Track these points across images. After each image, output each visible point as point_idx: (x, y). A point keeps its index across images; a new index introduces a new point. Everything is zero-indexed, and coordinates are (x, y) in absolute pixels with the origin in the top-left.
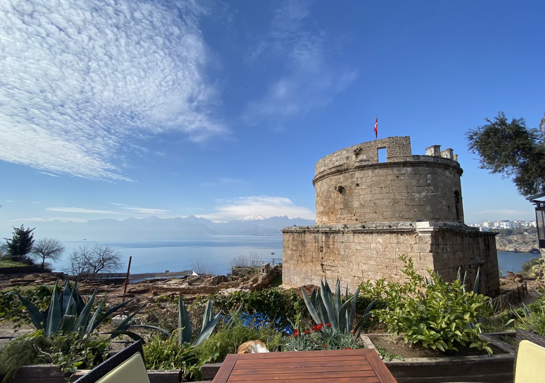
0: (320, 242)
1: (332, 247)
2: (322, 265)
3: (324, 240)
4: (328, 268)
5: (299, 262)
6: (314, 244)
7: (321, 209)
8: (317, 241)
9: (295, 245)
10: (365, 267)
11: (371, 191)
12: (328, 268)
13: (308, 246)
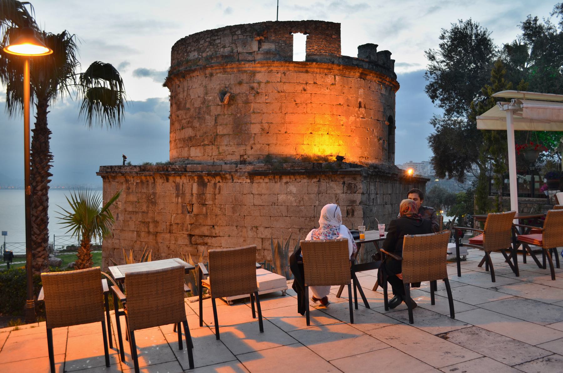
1: (211, 202)
2: (191, 236)
3: (195, 191)
4: (200, 240)
5: (143, 234)
6: (174, 200)
9: (132, 203)
11: (281, 108)
12: (200, 240)
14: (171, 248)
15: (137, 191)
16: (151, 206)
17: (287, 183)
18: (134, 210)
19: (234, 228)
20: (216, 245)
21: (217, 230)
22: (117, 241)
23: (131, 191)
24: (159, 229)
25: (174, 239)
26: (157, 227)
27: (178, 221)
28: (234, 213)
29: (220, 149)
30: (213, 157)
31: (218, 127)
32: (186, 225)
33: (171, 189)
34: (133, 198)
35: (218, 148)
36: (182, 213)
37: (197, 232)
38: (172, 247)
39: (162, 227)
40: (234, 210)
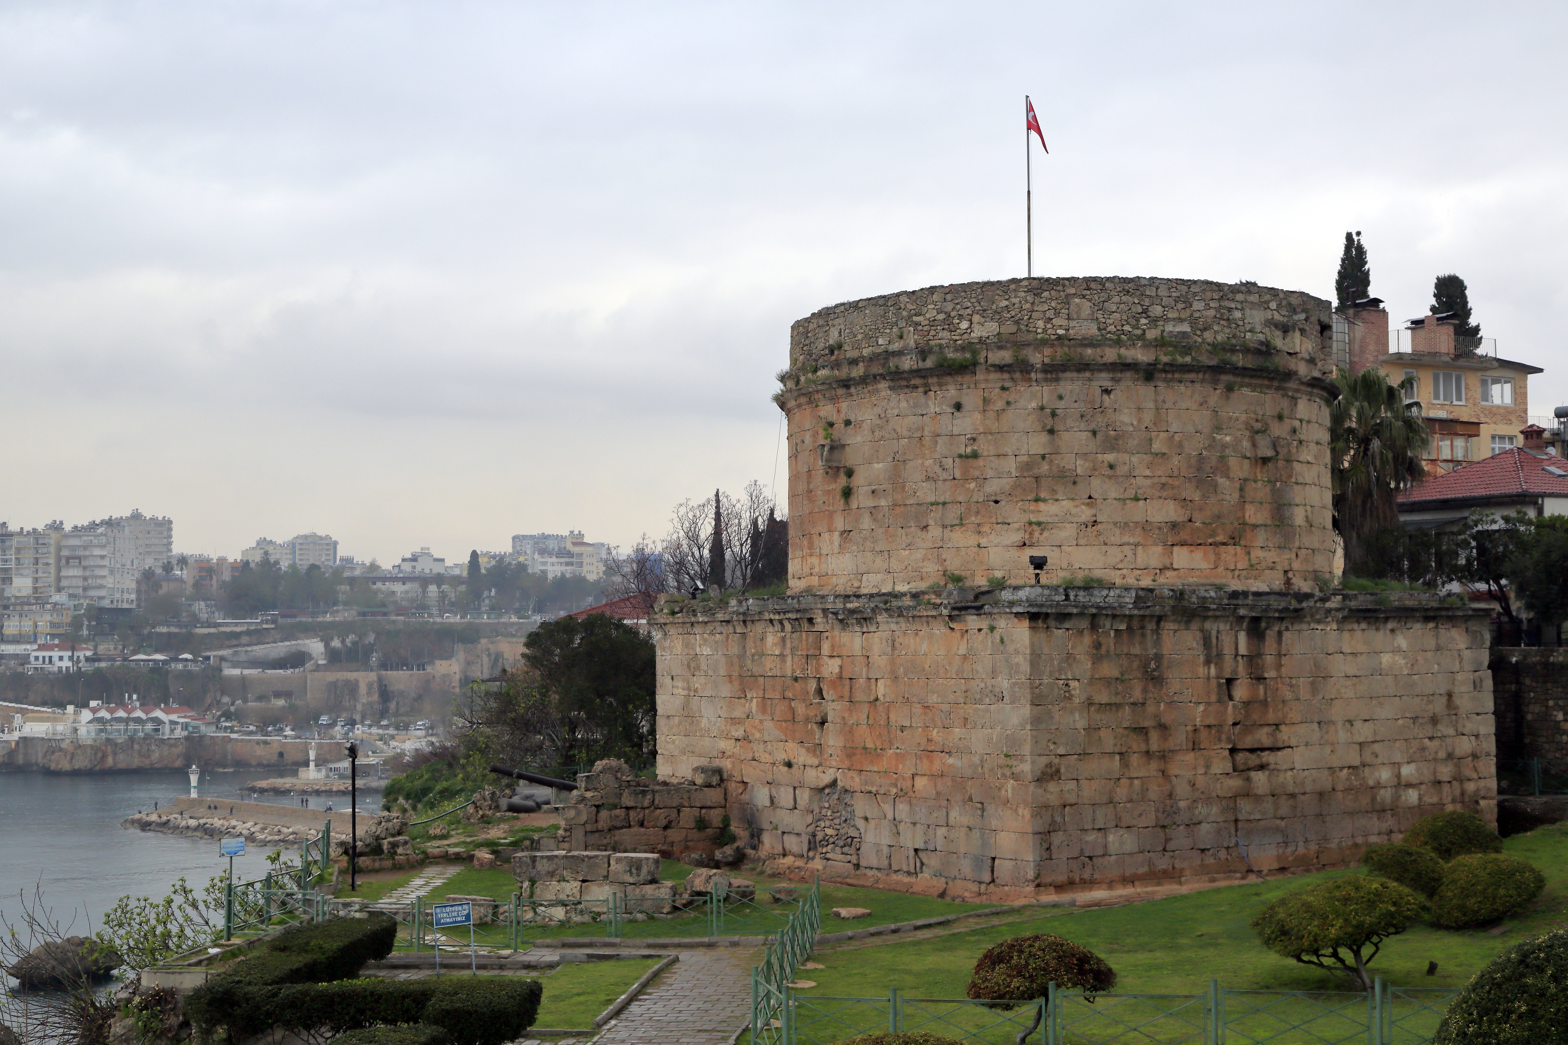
0: (1228, 659)
2: (1233, 751)
3: (1243, 649)
5: (1134, 759)
6: (1201, 671)
7: (1165, 511)
8: (1212, 655)
9: (1108, 682)
10: (1364, 732)
12: (1253, 760)
13: (1175, 681)
14: (1197, 786)
15: (1119, 652)
16: (1151, 687)
17: (1392, 631)
18: (1114, 700)
19: (1316, 724)
20: (1284, 767)
21: (1285, 735)
22: (1072, 785)
23: (1103, 650)
24: (1171, 744)
25: (1202, 762)
26: (1166, 739)
27: (1211, 721)
28: (1314, 695)
29: (1253, 556)
30: (1237, 573)
31: (1247, 506)
32: (1226, 728)
33: (1195, 645)
34: (1109, 670)
35: (1249, 553)
36: (1219, 701)
37: (1248, 741)
38: (1201, 781)
39: (1179, 738)
40: (1314, 688)
